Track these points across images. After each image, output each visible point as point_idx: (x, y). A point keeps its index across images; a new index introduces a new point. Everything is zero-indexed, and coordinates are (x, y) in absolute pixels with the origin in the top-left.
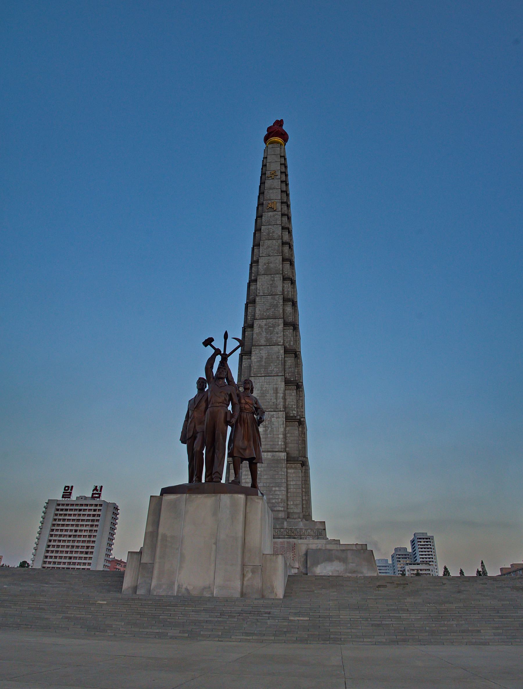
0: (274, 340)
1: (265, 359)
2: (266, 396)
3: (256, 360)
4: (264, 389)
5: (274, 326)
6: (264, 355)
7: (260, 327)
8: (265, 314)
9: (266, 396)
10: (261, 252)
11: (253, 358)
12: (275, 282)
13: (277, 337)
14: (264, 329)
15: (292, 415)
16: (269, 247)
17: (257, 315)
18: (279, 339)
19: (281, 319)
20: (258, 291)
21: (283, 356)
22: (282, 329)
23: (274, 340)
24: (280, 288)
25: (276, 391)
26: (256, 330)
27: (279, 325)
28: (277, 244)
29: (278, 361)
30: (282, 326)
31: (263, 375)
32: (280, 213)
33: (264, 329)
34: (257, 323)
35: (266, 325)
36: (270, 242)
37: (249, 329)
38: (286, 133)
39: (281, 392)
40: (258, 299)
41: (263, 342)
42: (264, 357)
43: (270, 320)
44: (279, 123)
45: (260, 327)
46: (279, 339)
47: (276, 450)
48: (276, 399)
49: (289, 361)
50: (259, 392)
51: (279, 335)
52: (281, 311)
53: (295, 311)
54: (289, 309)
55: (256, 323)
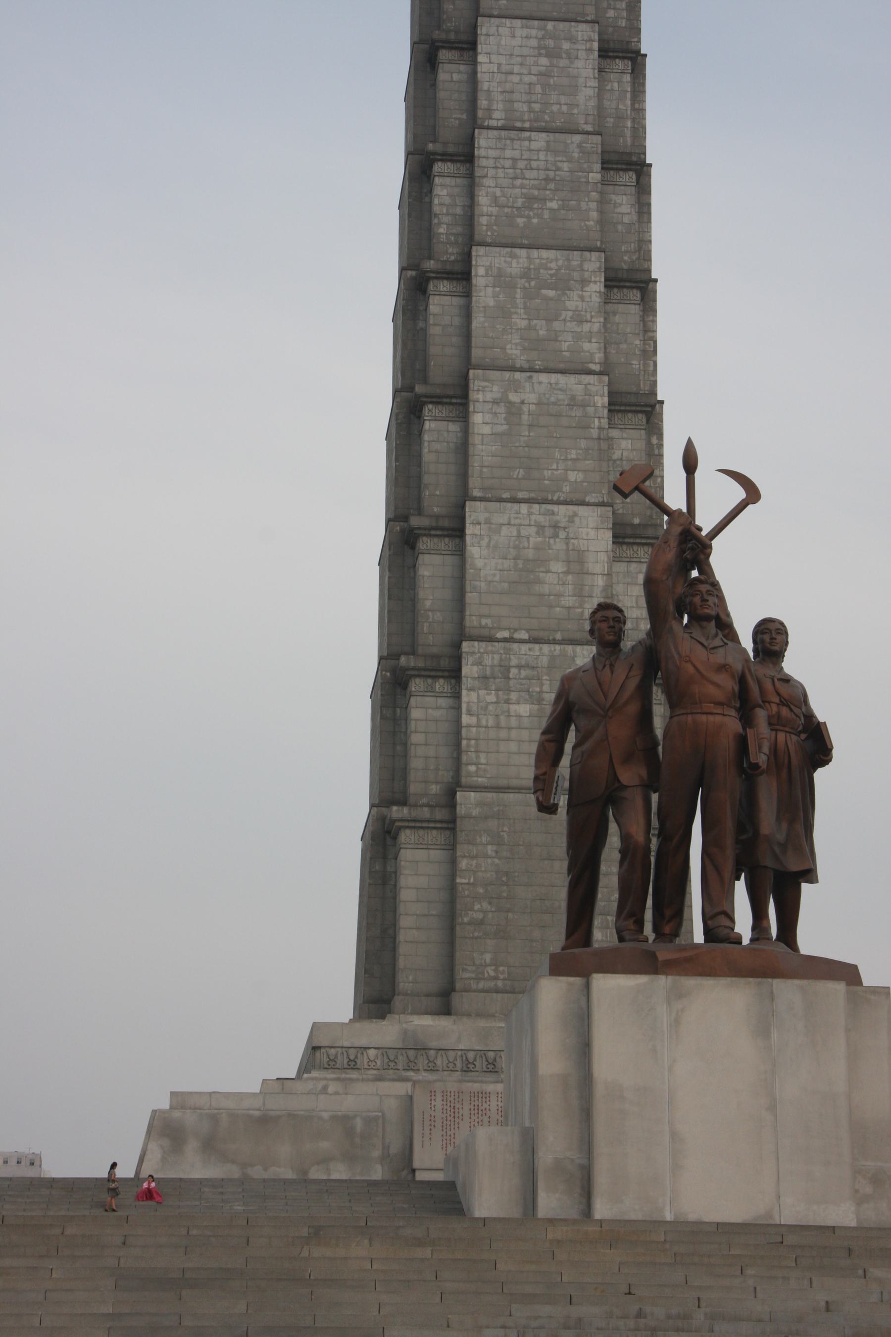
0: (565, 346)
1: (531, 426)
2: (539, 582)
4: (530, 554)
5: (562, 284)
7: (500, 279)
9: (539, 582)
11: (477, 419)
13: (578, 337)
14: (519, 294)
17: (484, 220)
18: (586, 346)
19: (595, 255)
20: (483, 103)
21: (604, 422)
22: (596, 299)
23: (565, 346)
24: (586, 95)
27: (584, 282)
29: (583, 444)
30: (597, 286)
31: (521, 495)
33: (519, 294)
40: (484, 142)
41: (515, 352)
42: (525, 417)
43: (545, 254)
45: (500, 279)
46: (586, 346)
49: (624, 444)
50: (507, 564)
51: (586, 327)
52: (594, 215)
54: (623, 204)
55: (484, 262)
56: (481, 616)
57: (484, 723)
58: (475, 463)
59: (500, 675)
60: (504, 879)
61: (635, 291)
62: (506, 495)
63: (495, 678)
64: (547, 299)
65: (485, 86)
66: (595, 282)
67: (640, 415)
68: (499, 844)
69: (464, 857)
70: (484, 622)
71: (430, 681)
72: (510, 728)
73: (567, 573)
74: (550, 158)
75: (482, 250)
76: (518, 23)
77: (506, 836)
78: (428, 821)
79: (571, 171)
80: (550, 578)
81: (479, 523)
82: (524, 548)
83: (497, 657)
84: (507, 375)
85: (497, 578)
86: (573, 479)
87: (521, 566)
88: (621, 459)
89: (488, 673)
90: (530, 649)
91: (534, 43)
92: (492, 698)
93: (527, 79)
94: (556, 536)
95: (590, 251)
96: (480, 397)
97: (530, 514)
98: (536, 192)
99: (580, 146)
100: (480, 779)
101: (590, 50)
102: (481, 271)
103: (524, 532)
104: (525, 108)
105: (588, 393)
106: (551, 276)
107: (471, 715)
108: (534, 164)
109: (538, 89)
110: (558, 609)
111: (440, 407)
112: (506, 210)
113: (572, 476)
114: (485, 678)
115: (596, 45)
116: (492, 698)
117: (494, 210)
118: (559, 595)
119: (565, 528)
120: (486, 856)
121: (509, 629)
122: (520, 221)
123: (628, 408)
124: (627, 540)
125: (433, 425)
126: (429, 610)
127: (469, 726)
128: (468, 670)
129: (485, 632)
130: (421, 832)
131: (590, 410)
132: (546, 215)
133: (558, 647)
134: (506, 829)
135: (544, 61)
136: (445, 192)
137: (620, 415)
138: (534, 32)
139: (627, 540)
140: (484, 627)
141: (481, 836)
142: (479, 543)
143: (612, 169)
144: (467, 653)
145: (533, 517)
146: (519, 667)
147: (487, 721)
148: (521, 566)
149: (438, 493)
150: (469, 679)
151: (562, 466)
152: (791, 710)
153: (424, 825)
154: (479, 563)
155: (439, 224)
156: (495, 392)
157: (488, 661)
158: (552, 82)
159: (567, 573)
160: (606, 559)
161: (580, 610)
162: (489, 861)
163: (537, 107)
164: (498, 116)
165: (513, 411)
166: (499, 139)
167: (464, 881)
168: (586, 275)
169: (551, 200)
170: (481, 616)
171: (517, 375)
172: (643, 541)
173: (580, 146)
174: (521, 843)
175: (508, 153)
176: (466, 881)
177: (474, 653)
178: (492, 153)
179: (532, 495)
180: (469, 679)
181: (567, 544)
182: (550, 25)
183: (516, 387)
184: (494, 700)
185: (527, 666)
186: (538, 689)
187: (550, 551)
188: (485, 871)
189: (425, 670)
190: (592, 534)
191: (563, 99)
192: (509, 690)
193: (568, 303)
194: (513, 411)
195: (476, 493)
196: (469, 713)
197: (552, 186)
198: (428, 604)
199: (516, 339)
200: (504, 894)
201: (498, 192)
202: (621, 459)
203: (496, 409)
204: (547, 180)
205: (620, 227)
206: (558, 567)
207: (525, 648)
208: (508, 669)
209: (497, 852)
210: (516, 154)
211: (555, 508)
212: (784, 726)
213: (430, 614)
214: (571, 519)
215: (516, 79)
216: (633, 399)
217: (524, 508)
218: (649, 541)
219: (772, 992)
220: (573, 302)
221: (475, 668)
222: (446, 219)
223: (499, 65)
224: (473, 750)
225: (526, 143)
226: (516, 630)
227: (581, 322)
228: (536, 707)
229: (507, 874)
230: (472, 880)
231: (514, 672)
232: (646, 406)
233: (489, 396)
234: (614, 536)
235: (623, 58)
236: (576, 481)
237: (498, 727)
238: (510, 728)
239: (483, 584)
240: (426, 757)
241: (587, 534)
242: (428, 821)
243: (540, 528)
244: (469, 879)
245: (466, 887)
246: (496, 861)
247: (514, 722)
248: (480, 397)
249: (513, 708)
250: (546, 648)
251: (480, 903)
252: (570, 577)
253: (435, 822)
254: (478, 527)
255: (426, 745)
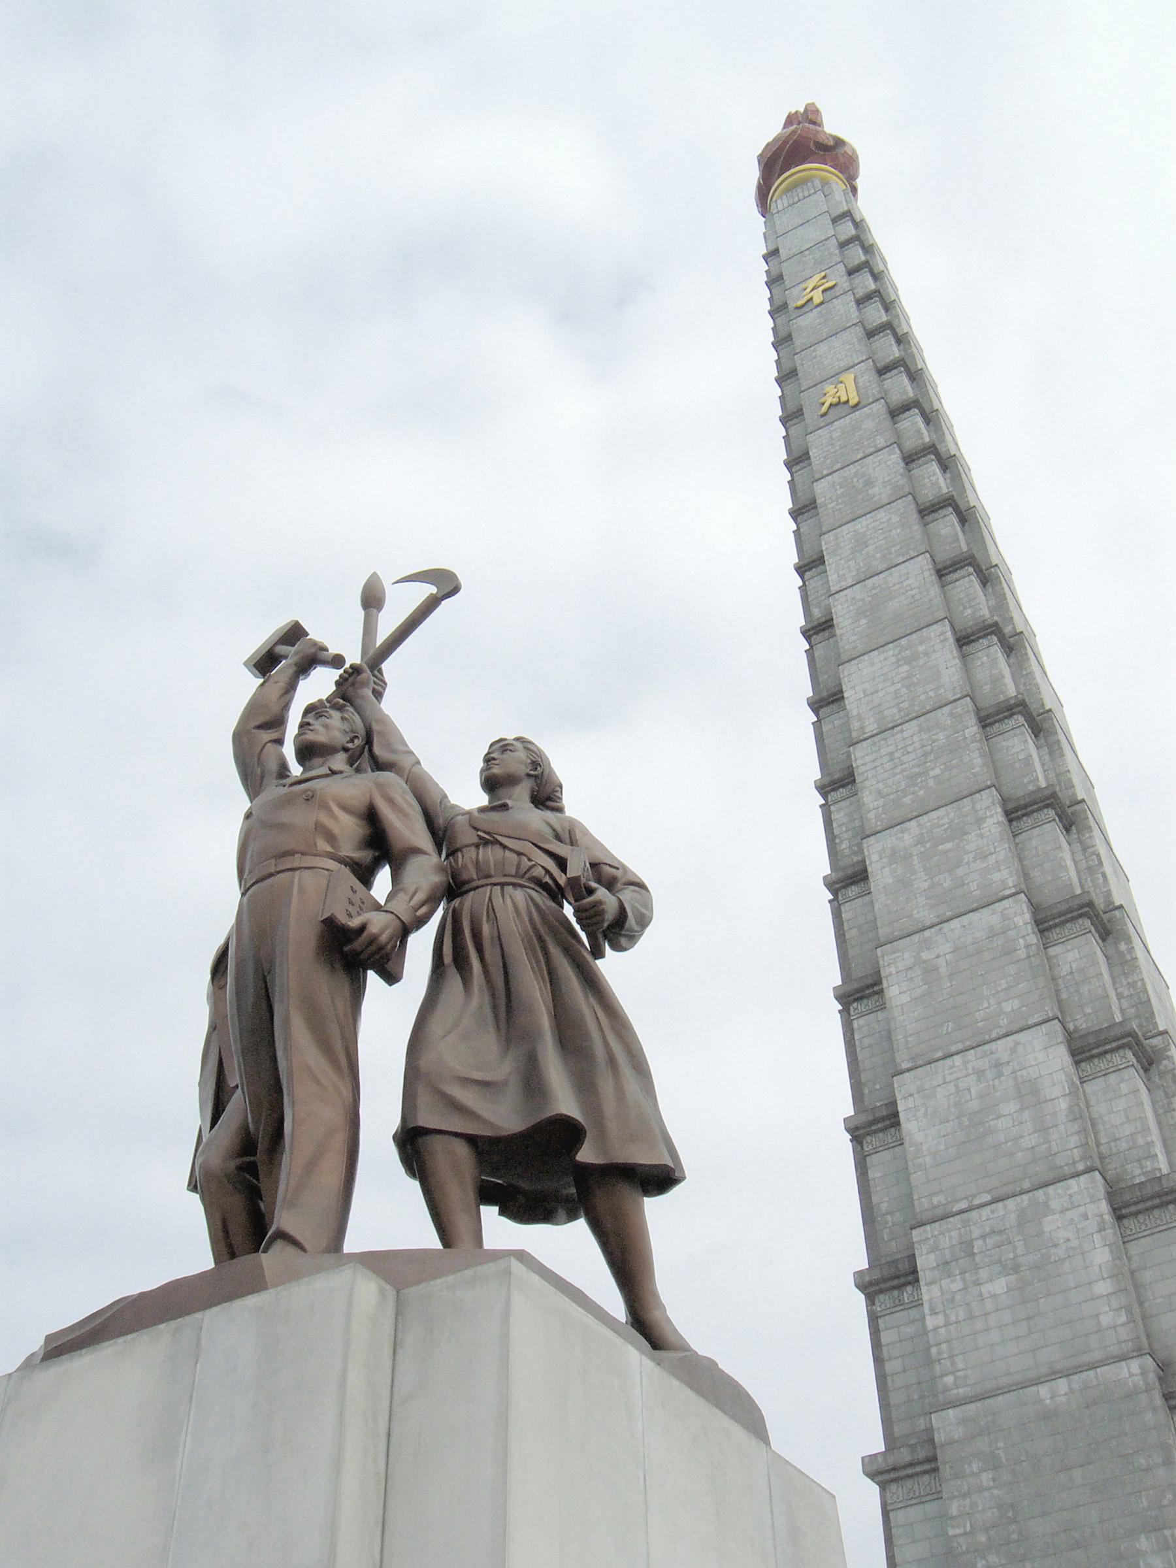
0: (973, 886)
1: (951, 976)
3: (905, 998)
4: (974, 1105)
5: (958, 833)
6: (941, 962)
7: (894, 856)
8: (907, 800)
10: (832, 577)
12: (921, 662)
15: (1143, 1179)
16: (861, 543)
17: (872, 815)
18: (996, 876)
19: (984, 794)
20: (855, 725)
22: (996, 830)
23: (973, 886)
25: (1030, 1094)
26: (881, 875)
27: (979, 821)
28: (895, 519)
29: (1012, 969)
31: (953, 1049)
32: (879, 407)
34: (879, 847)
35: (920, 841)
36: (861, 525)
37: (853, 891)
38: (839, 142)
39: (1056, 1092)
42: (943, 970)
43: (934, 815)
44: (811, 116)
45: (894, 856)
46: (996, 876)
47: (1097, 1355)
48: (1043, 1129)
49: (1070, 956)
51: (992, 859)
53: (1051, 753)
56: (931, 1195)
57: (953, 1318)
58: (899, 1037)
59: (963, 1254)
60: (1010, 1514)
61: (1045, 811)
62: (939, 1054)
63: (956, 1260)
64: (945, 852)
65: (855, 713)
66: (991, 816)
67: (1080, 921)
68: (995, 1469)
69: (954, 1497)
70: (935, 1200)
71: (896, 1293)
72: (986, 1314)
73: (1022, 1109)
74: (925, 736)
75: (872, 840)
76: (876, 653)
77: (1002, 1455)
78: (911, 1465)
79: (947, 737)
80: (1002, 1123)
81: (911, 1095)
82: (967, 1102)
83: (954, 1234)
84: (916, 937)
85: (942, 1147)
86: (1009, 1009)
87: (967, 1123)
88: (1072, 973)
89: (948, 1257)
90: (992, 1212)
91: (893, 660)
92: (957, 1285)
93: (892, 689)
94: (1000, 1074)
95: (979, 791)
96: (893, 970)
97: (966, 1062)
98: (917, 770)
99: (951, 714)
100: (961, 1391)
101: (945, 640)
102: (875, 857)
103: (962, 1085)
104: (895, 710)
105: (1005, 918)
106: (945, 830)
107: (936, 1313)
108: (910, 749)
109: (904, 690)
110: (1020, 1154)
111: (865, 1001)
112: (892, 797)
113: (1007, 1007)
114: (947, 1263)
115: (949, 634)
116: (957, 1285)
117: (881, 802)
118: (1016, 1139)
119: (1008, 1063)
120: (981, 1489)
121: (966, 1198)
122: (907, 800)
123: (1063, 918)
124: (1095, 1052)
125: (862, 1021)
126: (887, 1214)
127: (936, 1329)
128: (925, 1261)
129: (939, 1212)
130: (909, 1483)
131: (1012, 933)
132: (931, 783)
133: (1025, 1197)
134: (1001, 1444)
135: (906, 668)
136: (842, 814)
137: (1058, 930)
138: (891, 653)
139: (1095, 1052)
140: (937, 1207)
141: (970, 1465)
142: (914, 1116)
143: (996, 722)
144: (919, 1242)
145: (970, 1066)
146: (983, 1237)
147: (957, 1316)
148: (967, 1123)
149: (878, 1087)
150: (928, 1273)
151: (992, 1001)
152: (505, 847)
153: (910, 1471)
154: (918, 1137)
155: (841, 842)
156: (907, 957)
157: (945, 1242)
158: (915, 680)
159: (1022, 1109)
160: (1064, 1078)
161: (1044, 1146)
162: (986, 1494)
163: (905, 705)
164: (871, 727)
165: (930, 971)
166: (874, 744)
167: (958, 1531)
168: (981, 813)
169: (933, 769)
170: (931, 1195)
171: (927, 933)
172: (1114, 1045)
173: (951, 714)
174: (1023, 1458)
175: (884, 751)
176: (962, 1531)
177: (927, 1239)
178: (867, 759)
179: (968, 1043)
180: (928, 1273)
181: (1015, 1079)
182: (903, 642)
183: (928, 945)
184: (961, 1286)
185: (994, 1232)
186: (1011, 1255)
187: (997, 1094)
188: (984, 1510)
189: (885, 1280)
190: (1041, 1056)
191: (928, 688)
192: (977, 1268)
193: (967, 847)
194: (930, 971)
195: (905, 1066)
196: (934, 1312)
197: (932, 757)
198: (884, 1207)
199: (922, 900)
200: (1015, 1536)
201: (881, 786)
202: (1072, 973)
203: (910, 974)
204: (925, 755)
205: (1017, 765)
206: (1011, 1107)
207: (985, 1212)
208: (970, 1243)
209: (994, 1480)
210: (892, 748)
211: (993, 1046)
212: (490, 876)
213: (889, 1218)
214: (1013, 1051)
215: (881, 694)
216: (1064, 907)
217: (958, 1060)
218: (1121, 1042)
219: (198, 1345)
220: (973, 842)
221: (932, 1257)
222: (846, 836)
223: (864, 691)
224: (945, 1355)
225: (899, 736)
226: (974, 1196)
227: (985, 857)
228: (1013, 1278)
229: (1012, 1506)
230: (968, 1529)
231: (978, 1245)
232: (1081, 907)
233: (901, 965)
234: (1073, 1053)
235: (985, 636)
236: (1013, 1010)
237: (971, 1317)
238: (986, 1314)
239: (928, 1159)
240: (907, 1387)
241: (1036, 1059)
242: (911, 1465)
243: (980, 1073)
244: (965, 1527)
245: (961, 1540)
246: (995, 1491)
247: (989, 1305)
248: (893, 970)
249: (985, 1289)
250: (1011, 1203)
251: (984, 1558)
252: (1026, 1114)
253: (920, 1463)
254: (911, 1099)
255: (904, 1371)
